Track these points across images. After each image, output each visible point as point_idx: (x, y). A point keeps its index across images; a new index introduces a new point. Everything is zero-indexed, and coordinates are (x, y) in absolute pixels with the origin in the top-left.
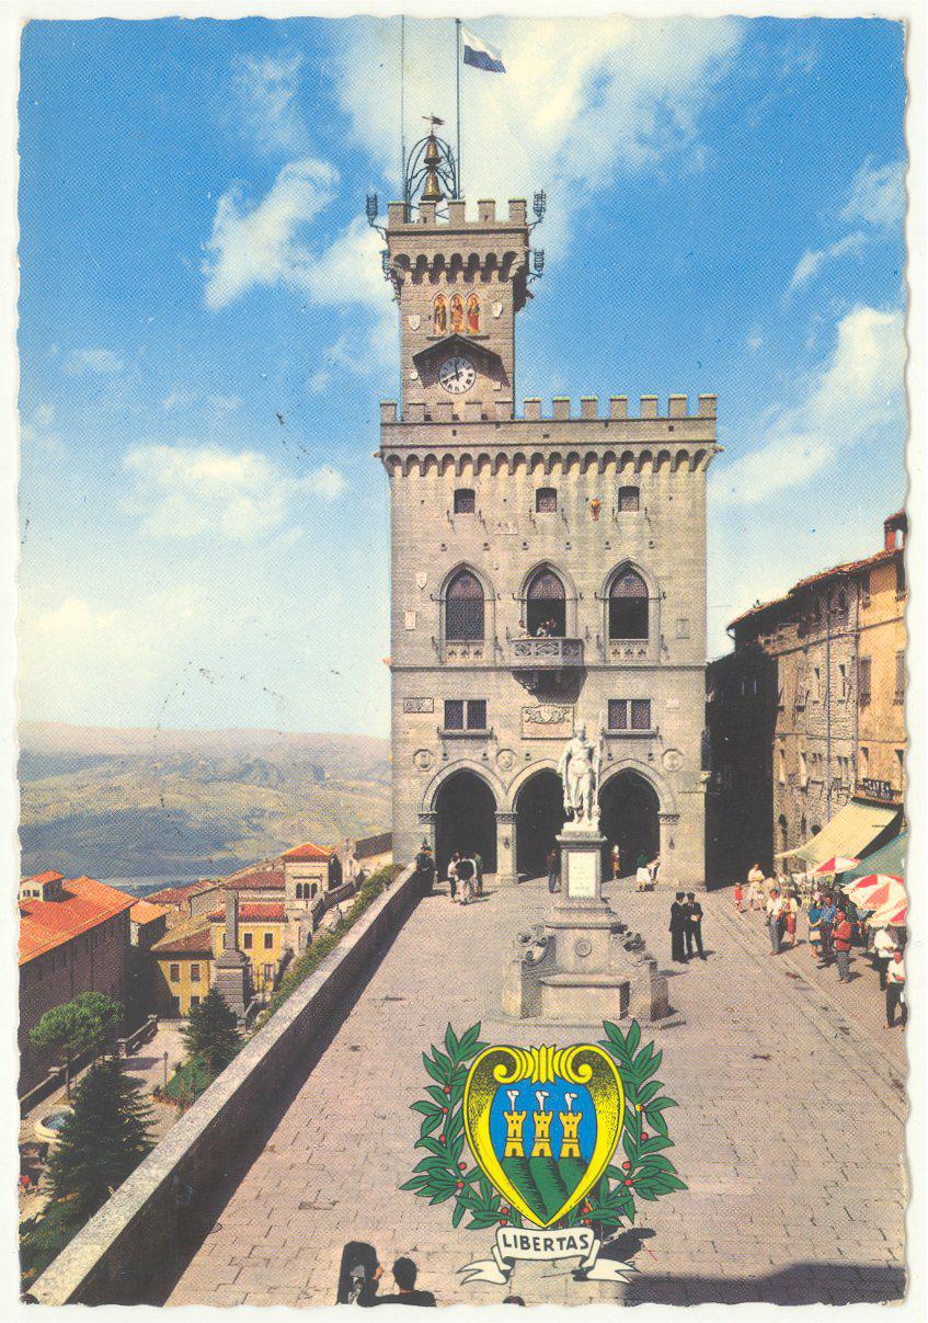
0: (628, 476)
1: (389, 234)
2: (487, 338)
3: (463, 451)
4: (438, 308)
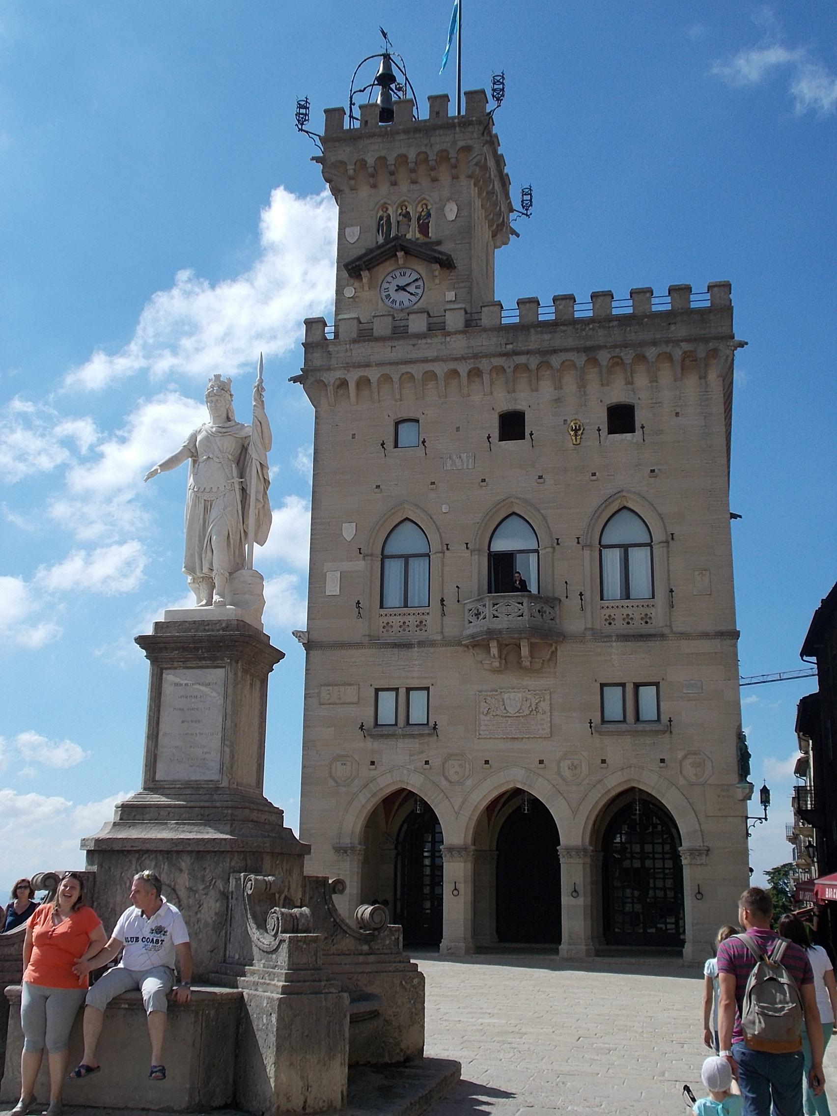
2: (439, 243)
3: (405, 369)
4: (381, 218)
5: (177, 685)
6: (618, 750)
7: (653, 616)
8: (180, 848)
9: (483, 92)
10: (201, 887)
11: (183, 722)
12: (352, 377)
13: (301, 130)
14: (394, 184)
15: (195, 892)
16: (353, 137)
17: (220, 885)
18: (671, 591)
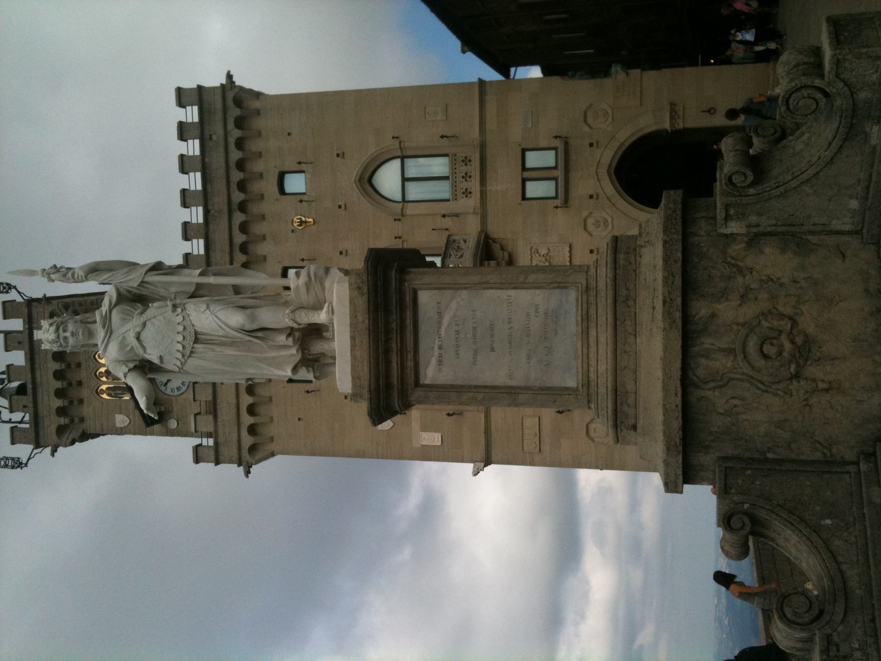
0: (269, 186)
1: (38, 445)
4: (109, 395)
5: (440, 362)
6: (582, 186)
7: (464, 155)
8: (678, 315)
9: (4, 303)
10: (740, 280)
11: (493, 350)
12: (247, 420)
13: (26, 465)
14: (80, 383)
15: (748, 289)
16: (36, 420)
17: (736, 249)
18: (442, 137)
